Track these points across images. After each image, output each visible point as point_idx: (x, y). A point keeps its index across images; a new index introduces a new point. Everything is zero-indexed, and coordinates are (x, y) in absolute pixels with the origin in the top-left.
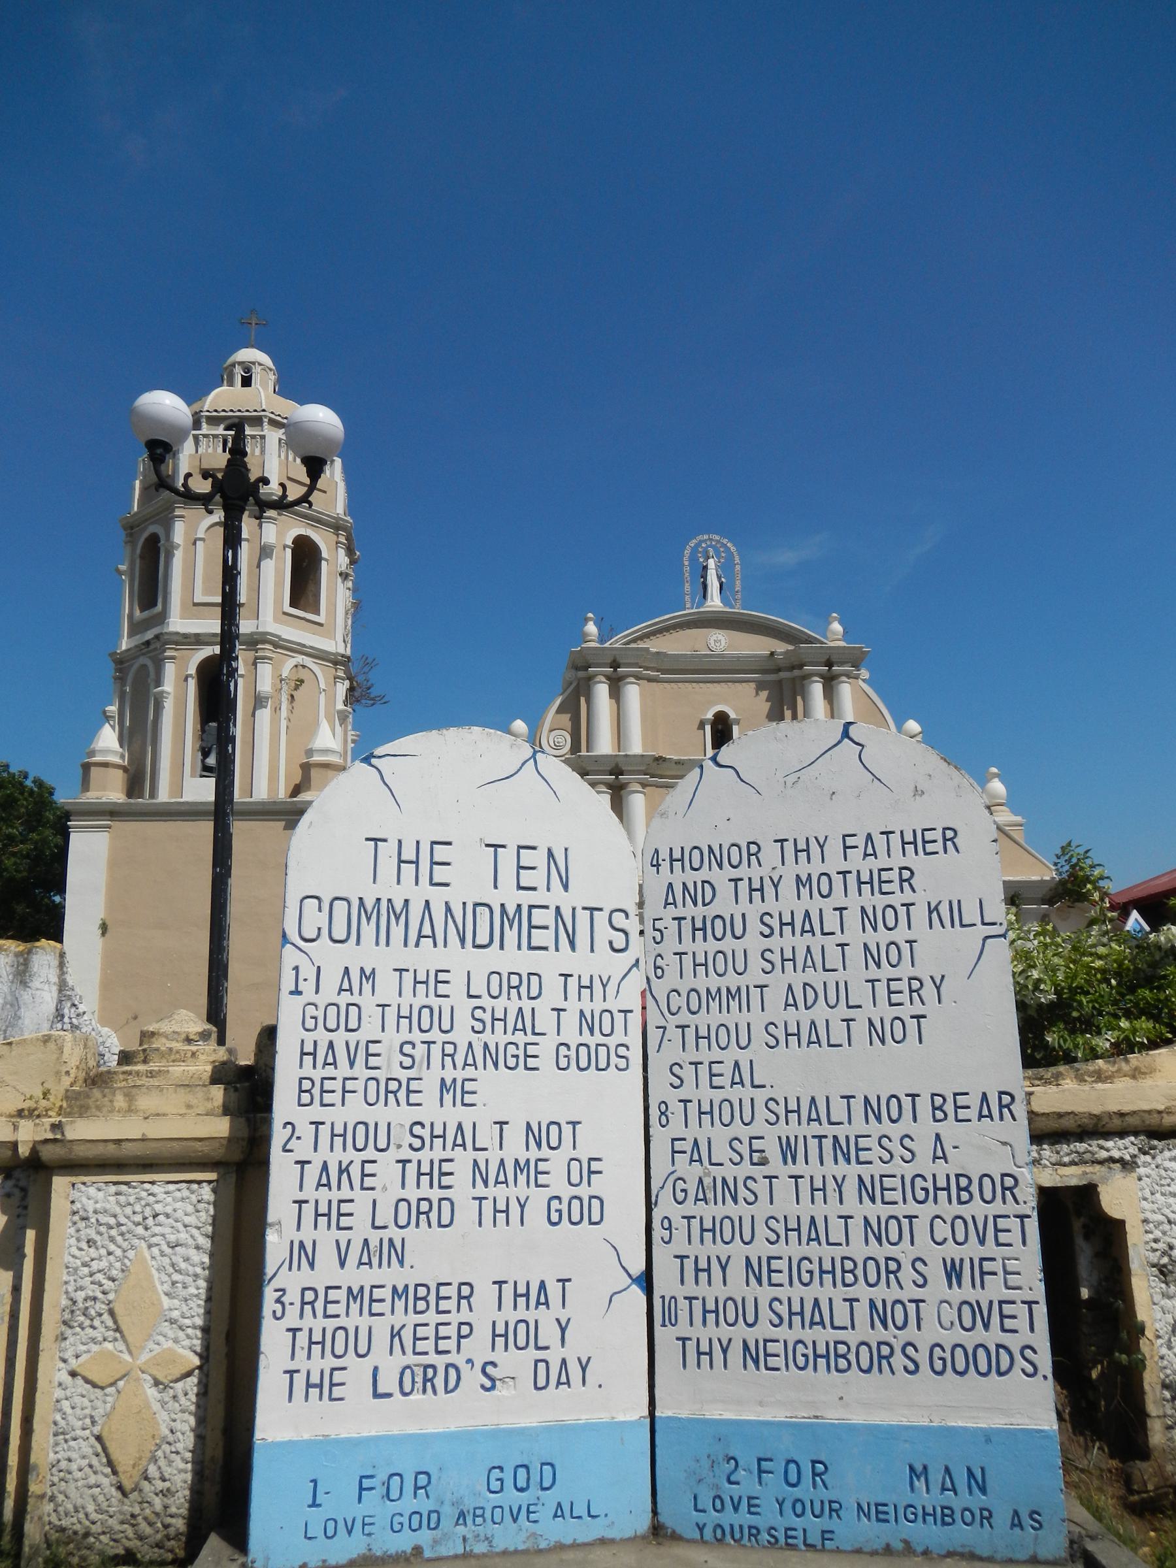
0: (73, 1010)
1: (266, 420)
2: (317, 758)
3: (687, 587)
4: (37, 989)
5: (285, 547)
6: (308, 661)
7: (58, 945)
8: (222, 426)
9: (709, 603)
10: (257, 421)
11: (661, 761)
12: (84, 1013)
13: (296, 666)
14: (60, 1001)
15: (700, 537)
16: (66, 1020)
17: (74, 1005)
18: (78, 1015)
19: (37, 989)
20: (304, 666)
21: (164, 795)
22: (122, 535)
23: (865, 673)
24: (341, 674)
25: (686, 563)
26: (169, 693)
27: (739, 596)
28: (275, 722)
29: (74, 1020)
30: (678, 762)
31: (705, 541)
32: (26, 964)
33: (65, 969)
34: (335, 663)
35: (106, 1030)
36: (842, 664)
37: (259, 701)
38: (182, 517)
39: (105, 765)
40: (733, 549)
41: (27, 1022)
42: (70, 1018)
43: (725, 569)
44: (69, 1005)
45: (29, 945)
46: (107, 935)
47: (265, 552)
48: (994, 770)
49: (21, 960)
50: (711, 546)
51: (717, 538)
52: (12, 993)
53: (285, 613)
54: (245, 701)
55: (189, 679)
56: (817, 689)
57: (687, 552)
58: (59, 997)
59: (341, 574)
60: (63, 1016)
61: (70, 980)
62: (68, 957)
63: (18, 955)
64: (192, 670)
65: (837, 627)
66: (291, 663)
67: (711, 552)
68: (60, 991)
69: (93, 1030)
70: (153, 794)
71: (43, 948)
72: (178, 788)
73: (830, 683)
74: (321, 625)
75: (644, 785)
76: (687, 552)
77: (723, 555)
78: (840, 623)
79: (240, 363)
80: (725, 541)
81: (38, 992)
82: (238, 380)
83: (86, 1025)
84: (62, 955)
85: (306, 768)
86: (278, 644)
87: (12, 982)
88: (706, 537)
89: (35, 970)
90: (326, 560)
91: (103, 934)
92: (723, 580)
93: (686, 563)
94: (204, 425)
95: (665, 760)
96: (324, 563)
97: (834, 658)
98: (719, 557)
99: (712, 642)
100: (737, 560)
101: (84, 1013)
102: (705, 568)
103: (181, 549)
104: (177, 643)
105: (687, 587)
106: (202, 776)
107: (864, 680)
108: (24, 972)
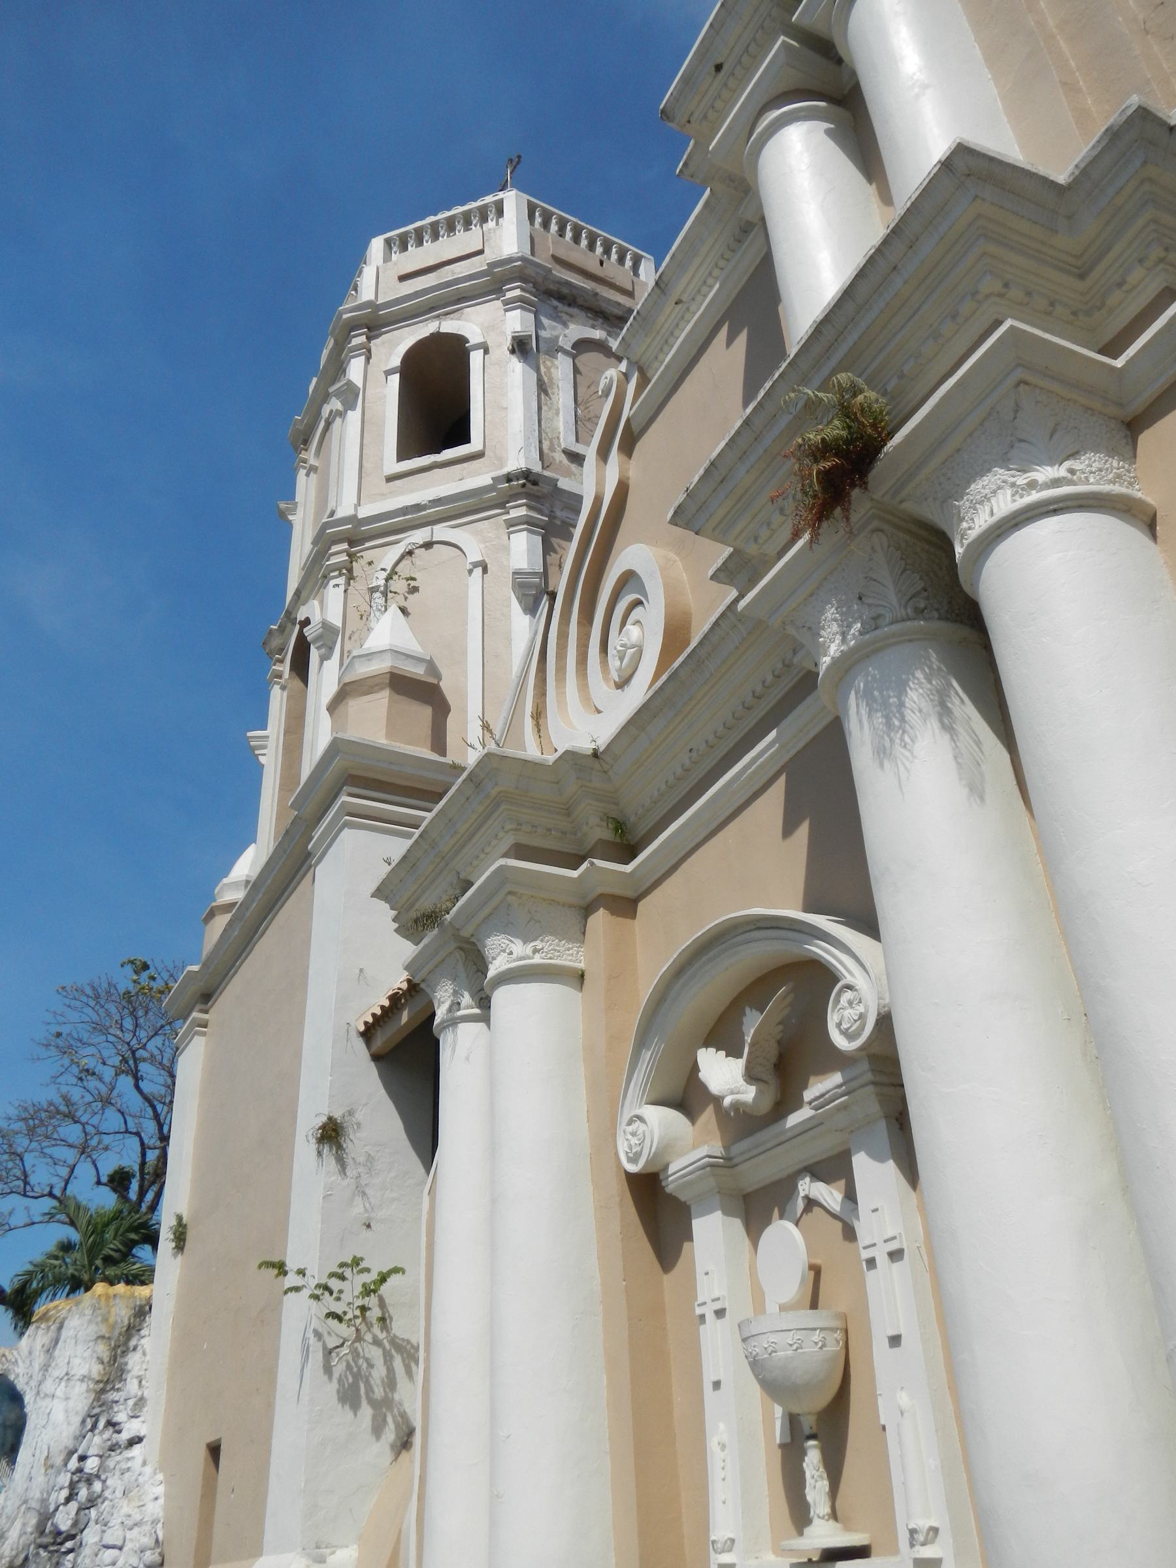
6: (441, 532)
12: (135, 1441)
13: (410, 553)
17: (110, 1424)
19: (46, 1395)
20: (428, 545)
26: (268, 737)
33: (132, 1343)
53: (390, 479)
66: (399, 550)
90: (477, 347)
101: (135, 1441)
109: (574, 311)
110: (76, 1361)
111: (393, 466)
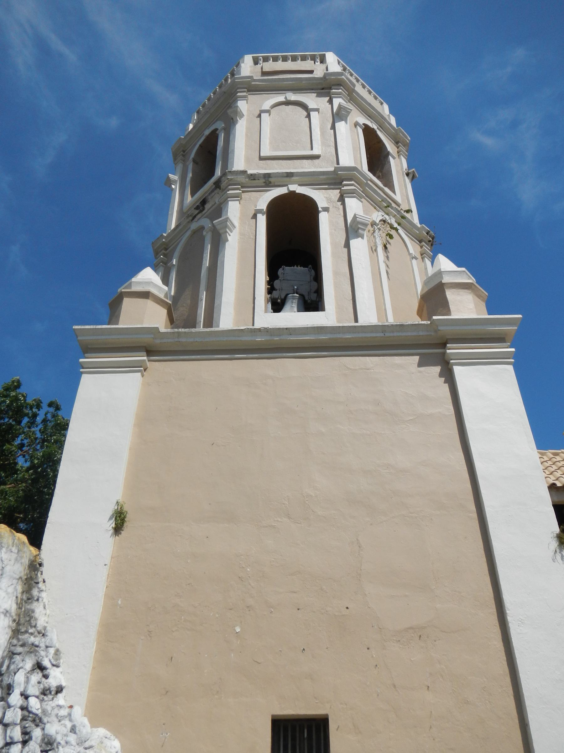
0: (36, 677)
17: (40, 667)
18: (45, 692)
29: (34, 704)
33: (35, 592)
35: (102, 731)
39: (146, 295)
42: (25, 696)
44: (29, 664)
46: (124, 533)
55: (259, 216)
58: (11, 644)
62: (47, 572)
68: (16, 632)
69: (73, 730)
70: (210, 321)
83: (60, 719)
91: (118, 530)
101: (59, 690)
103: (245, 117)
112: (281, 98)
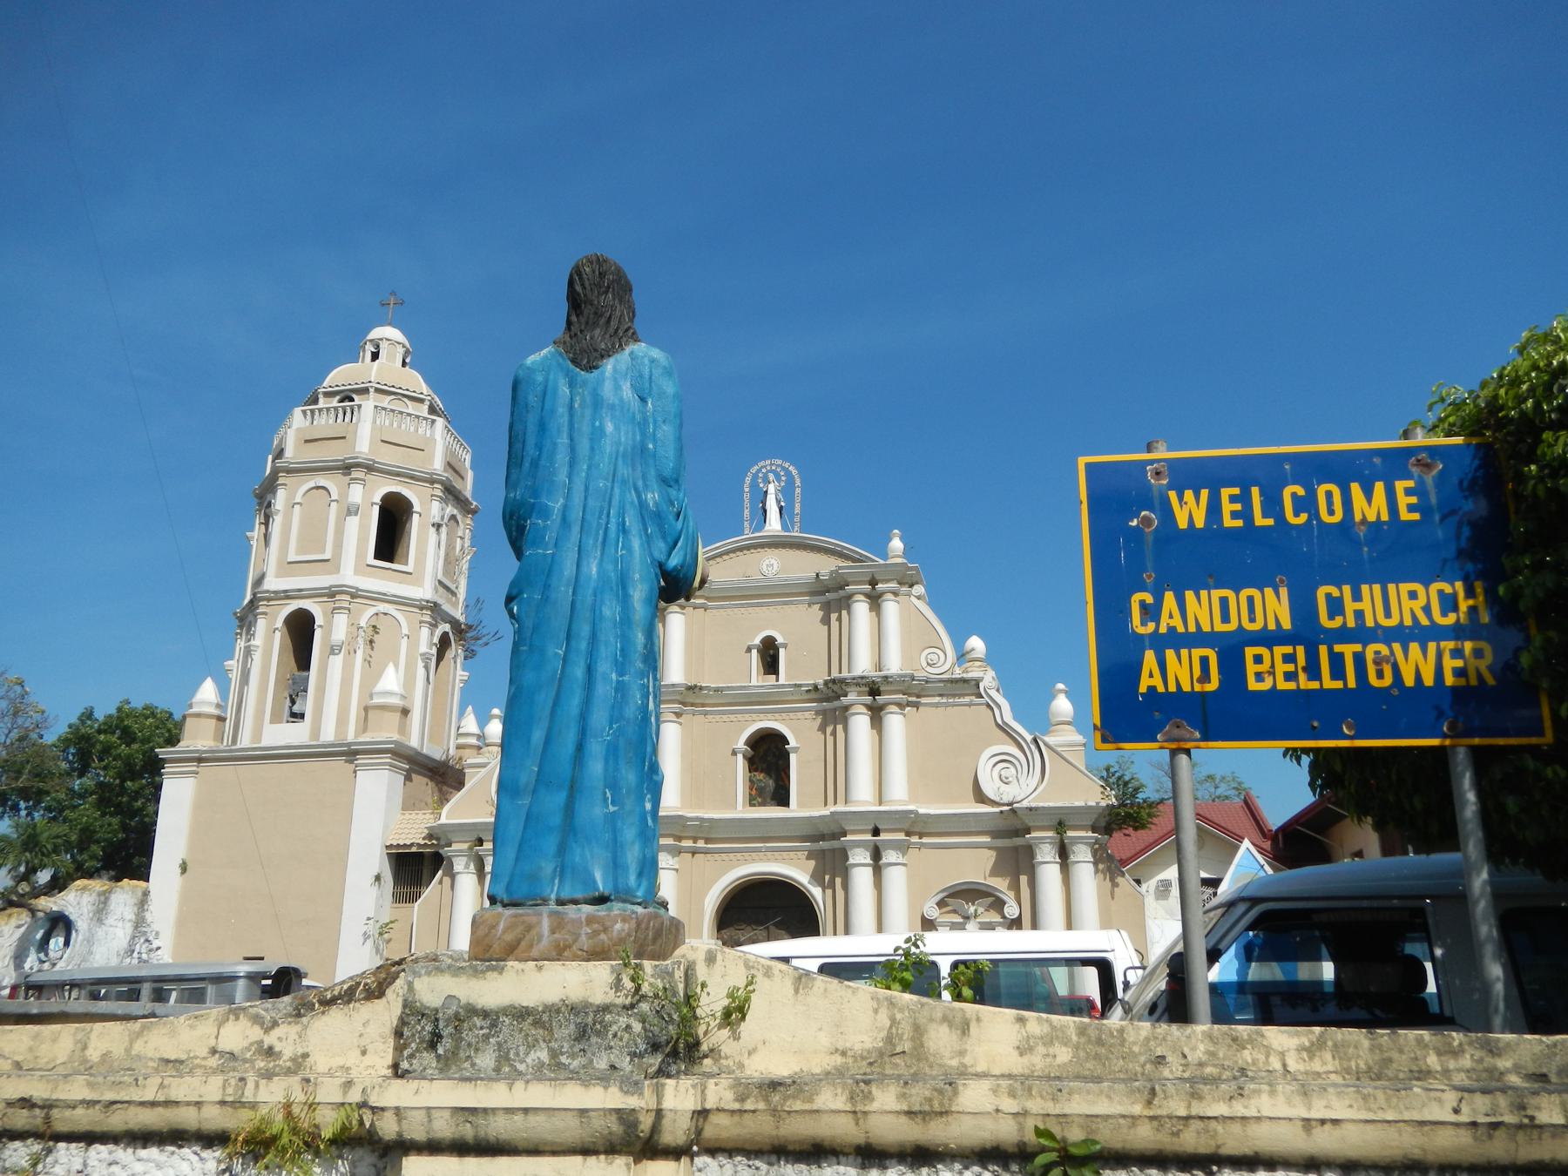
1: (372, 390)
2: (377, 700)
3: (746, 512)
4: (111, 926)
5: (373, 504)
7: (142, 884)
8: (338, 398)
9: (767, 527)
10: (365, 391)
11: (696, 690)
12: (158, 948)
14: (133, 938)
15: (762, 464)
16: (135, 955)
19: (111, 926)
20: (386, 614)
21: (245, 741)
22: (256, 501)
23: (919, 589)
24: (428, 619)
25: (747, 490)
27: (797, 519)
28: (348, 668)
29: (144, 956)
30: (717, 690)
31: (765, 467)
32: (106, 902)
33: (146, 907)
34: (422, 608)
36: (887, 581)
37: (333, 650)
38: (285, 485)
39: (198, 715)
40: (794, 471)
41: (97, 957)
43: (786, 492)
44: (142, 940)
45: (113, 884)
47: (352, 511)
48: (1061, 686)
49: (102, 898)
50: (771, 471)
51: (779, 462)
52: (90, 930)
53: (368, 565)
54: (322, 652)
56: (861, 608)
57: (748, 480)
59: (433, 525)
60: (133, 951)
61: (149, 916)
63: (99, 894)
64: (280, 623)
65: (897, 544)
66: (372, 611)
67: (771, 477)
68: (136, 927)
70: (234, 741)
71: (122, 888)
72: (258, 732)
73: (875, 600)
74: (411, 574)
75: (678, 715)
76: (748, 480)
77: (783, 478)
78: (901, 539)
79: (371, 341)
80: (787, 465)
81: (111, 929)
82: (368, 356)
84: (146, 894)
85: (366, 709)
86: (355, 594)
87: (92, 919)
88: (768, 462)
89: (111, 908)
90: (417, 513)
92: (783, 504)
93: (747, 490)
94: (321, 400)
95: (701, 688)
96: (415, 517)
97: (878, 577)
98: (779, 480)
99: (765, 567)
100: (798, 483)
101: (158, 948)
102: (766, 492)
104: (269, 600)
105: (746, 512)
106: (288, 722)
107: (919, 598)
108: (103, 909)
109: (450, 497)
110: (126, 913)
111: (371, 559)
112: (312, 484)
